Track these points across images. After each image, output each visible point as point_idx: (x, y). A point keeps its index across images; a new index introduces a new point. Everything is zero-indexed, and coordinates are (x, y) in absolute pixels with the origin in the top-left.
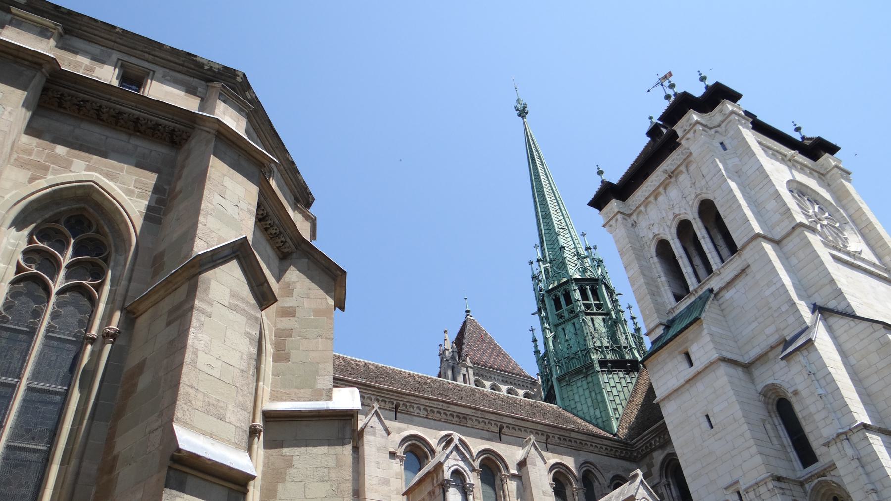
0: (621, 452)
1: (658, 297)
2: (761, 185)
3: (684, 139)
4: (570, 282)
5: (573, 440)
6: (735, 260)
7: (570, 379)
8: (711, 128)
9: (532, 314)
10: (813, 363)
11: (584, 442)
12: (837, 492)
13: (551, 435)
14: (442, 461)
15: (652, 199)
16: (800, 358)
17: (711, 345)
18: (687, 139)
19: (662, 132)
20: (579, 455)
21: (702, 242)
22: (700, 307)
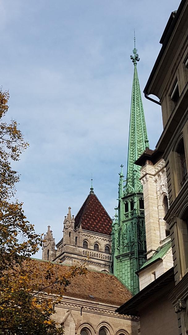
11: (104, 310)
20: (101, 318)
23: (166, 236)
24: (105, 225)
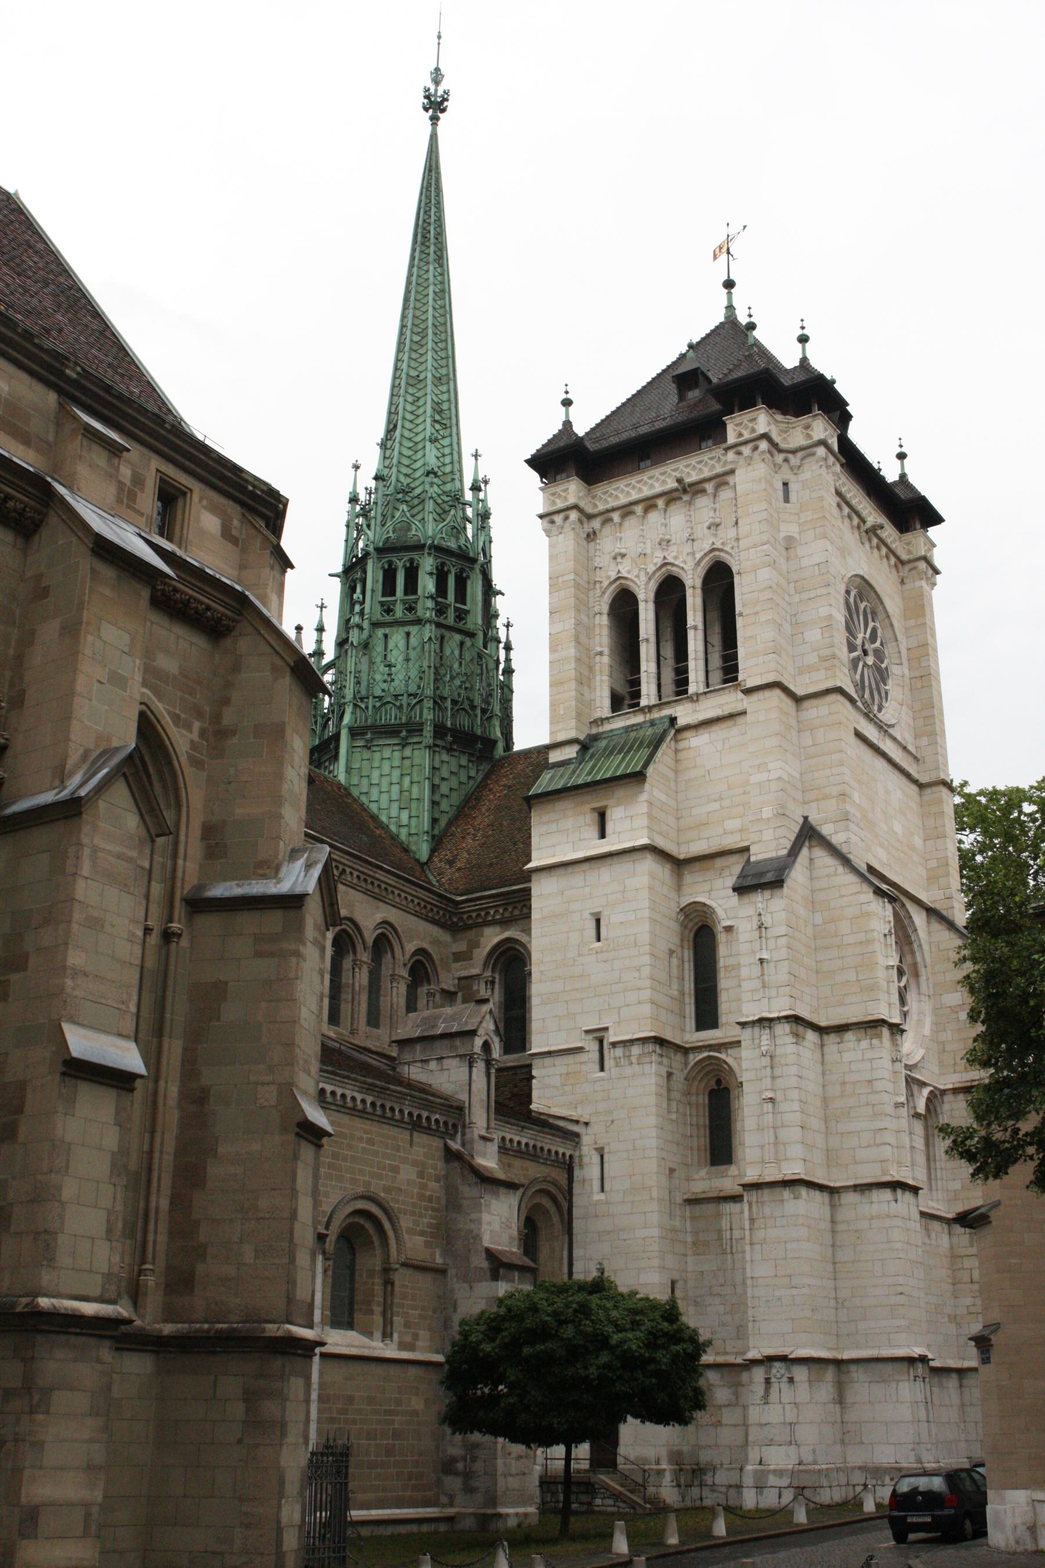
0: (438, 912)
1: (586, 688)
2: (812, 594)
4: (426, 551)
5: (376, 883)
6: (727, 691)
7: (372, 740)
8: (780, 451)
9: (330, 575)
10: (771, 913)
11: (390, 889)
13: (348, 870)
15: (639, 509)
16: (759, 900)
17: (644, 821)
18: (739, 453)
20: (377, 908)
21: (690, 634)
23: (613, 711)
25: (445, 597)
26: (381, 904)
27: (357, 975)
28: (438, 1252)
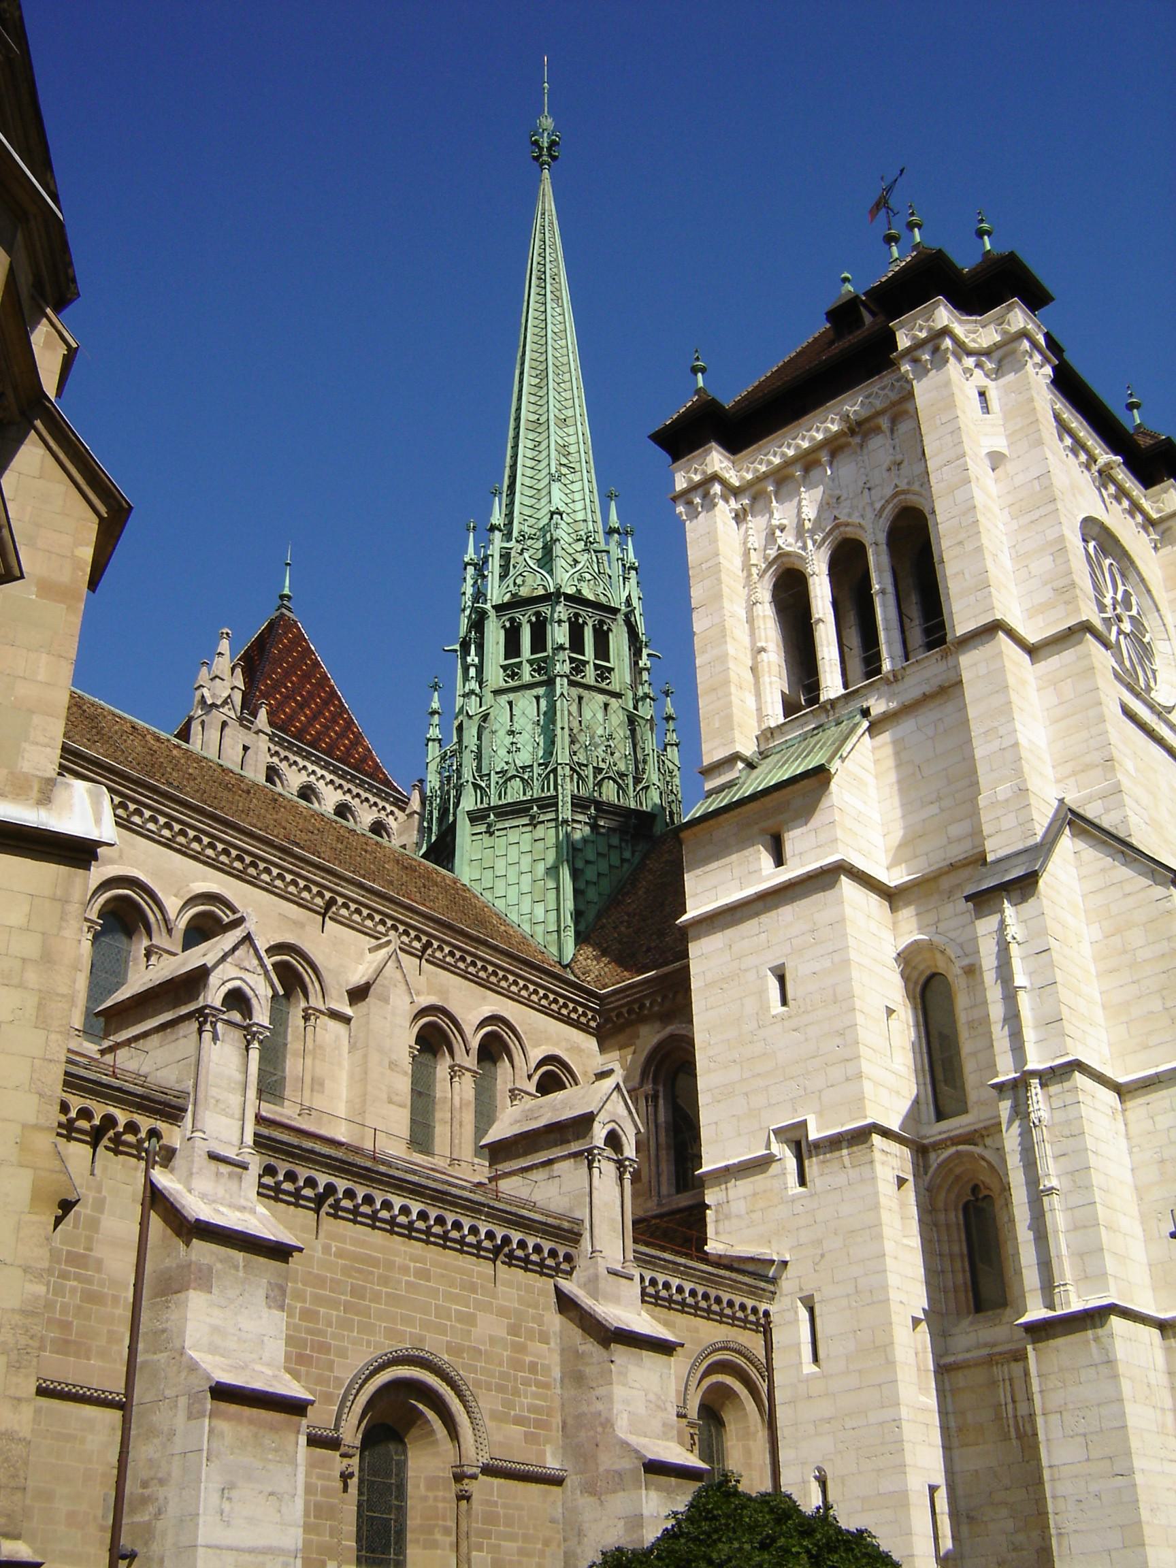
3: (909, 357)
8: (970, 353)
10: (1025, 921)
12: (985, 1177)
13: (435, 944)
14: (209, 965)
19: (859, 321)
20: (484, 998)
21: (877, 601)
22: (833, 743)
23: (786, 716)
24: (336, 732)
25: (584, 655)
26: (489, 993)
27: (456, 1085)
28: (549, 1449)
